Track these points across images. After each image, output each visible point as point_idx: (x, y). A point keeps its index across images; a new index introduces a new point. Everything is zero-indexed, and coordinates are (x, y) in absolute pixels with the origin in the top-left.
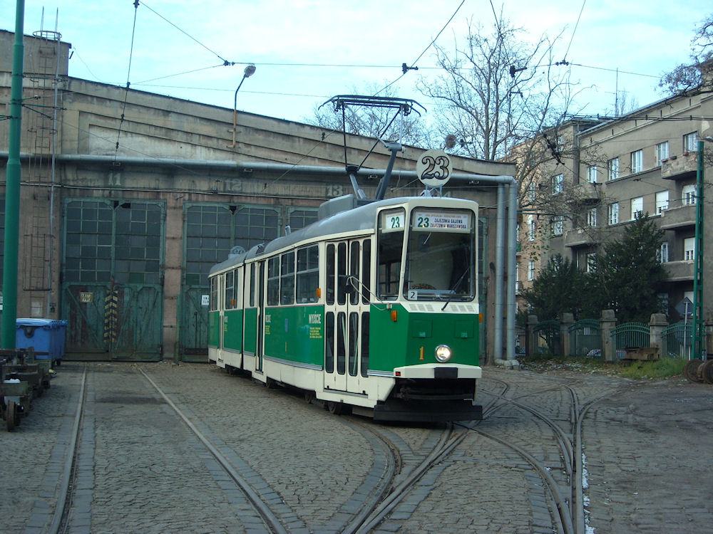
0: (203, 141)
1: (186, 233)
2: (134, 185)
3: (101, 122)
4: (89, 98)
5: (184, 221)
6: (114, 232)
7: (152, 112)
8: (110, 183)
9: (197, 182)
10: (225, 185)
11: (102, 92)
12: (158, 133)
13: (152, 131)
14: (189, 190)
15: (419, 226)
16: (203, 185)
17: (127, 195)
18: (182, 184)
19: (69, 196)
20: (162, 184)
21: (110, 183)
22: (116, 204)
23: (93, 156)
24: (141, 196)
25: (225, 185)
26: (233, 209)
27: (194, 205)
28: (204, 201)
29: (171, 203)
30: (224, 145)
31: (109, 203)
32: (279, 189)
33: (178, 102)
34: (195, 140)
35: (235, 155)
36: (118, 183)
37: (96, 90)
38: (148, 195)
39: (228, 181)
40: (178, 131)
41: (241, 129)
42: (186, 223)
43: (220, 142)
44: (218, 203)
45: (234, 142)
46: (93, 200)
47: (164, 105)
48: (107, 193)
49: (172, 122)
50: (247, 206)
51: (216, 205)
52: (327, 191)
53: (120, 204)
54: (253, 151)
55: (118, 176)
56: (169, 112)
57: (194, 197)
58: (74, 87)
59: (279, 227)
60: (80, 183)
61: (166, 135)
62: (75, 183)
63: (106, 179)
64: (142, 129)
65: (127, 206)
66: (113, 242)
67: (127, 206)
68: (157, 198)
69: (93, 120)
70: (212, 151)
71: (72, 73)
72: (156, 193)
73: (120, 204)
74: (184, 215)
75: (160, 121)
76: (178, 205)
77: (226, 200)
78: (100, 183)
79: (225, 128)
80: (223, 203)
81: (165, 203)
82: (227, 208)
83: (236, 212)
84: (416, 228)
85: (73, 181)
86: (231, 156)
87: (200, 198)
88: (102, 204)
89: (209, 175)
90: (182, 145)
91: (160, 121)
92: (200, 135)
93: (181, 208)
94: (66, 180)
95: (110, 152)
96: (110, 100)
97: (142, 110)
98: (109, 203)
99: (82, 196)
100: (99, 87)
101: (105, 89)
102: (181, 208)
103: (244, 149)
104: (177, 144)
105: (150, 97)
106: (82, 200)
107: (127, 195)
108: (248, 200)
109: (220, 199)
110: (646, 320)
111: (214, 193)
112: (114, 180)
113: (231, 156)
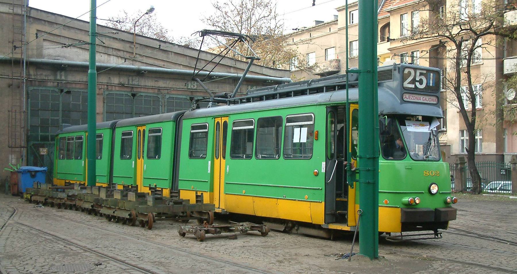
0: (115, 53)
1: (105, 111)
2: (74, 79)
3: (51, 38)
4: (43, 22)
5: (104, 103)
6: (61, 109)
8: (58, 78)
9: (112, 79)
10: (129, 80)
11: (52, 19)
14: (107, 83)
16: (116, 80)
17: (69, 86)
19: (32, 85)
21: (58, 78)
22: (62, 91)
23: (45, 60)
24: (78, 86)
25: (129, 80)
26: (134, 95)
27: (110, 92)
28: (115, 90)
30: (127, 56)
31: (57, 90)
32: (161, 84)
33: (100, 27)
34: (110, 52)
35: (134, 62)
36: (63, 78)
37: (48, 17)
38: (82, 86)
39: (130, 78)
41: (137, 46)
42: (105, 104)
43: (125, 53)
44: (125, 91)
45: (134, 54)
46: (48, 89)
48: (56, 84)
50: (142, 94)
51: (124, 93)
53: (65, 90)
54: (145, 60)
55: (63, 73)
57: (110, 88)
58: (33, 14)
59: (160, 106)
60: (39, 77)
62: (36, 77)
63: (56, 75)
65: (69, 92)
67: (69, 92)
69: (46, 36)
70: (120, 59)
71: (30, 6)
74: (104, 98)
76: (100, 93)
77: (129, 90)
78: (51, 77)
79: (128, 45)
80: (128, 92)
82: (130, 94)
83: (136, 98)
85: (34, 75)
86: (131, 62)
87: (114, 88)
88: (53, 91)
89: (119, 74)
90: (102, 54)
92: (113, 48)
93: (102, 94)
95: (57, 58)
96: (57, 24)
97: (78, 31)
98: (57, 90)
99: (40, 86)
100: (50, 15)
101: (53, 17)
102: (102, 94)
103: (139, 58)
105: (82, 23)
106: (40, 88)
107: (69, 86)
108: (142, 90)
109: (125, 89)
111: (122, 85)
112: (61, 76)
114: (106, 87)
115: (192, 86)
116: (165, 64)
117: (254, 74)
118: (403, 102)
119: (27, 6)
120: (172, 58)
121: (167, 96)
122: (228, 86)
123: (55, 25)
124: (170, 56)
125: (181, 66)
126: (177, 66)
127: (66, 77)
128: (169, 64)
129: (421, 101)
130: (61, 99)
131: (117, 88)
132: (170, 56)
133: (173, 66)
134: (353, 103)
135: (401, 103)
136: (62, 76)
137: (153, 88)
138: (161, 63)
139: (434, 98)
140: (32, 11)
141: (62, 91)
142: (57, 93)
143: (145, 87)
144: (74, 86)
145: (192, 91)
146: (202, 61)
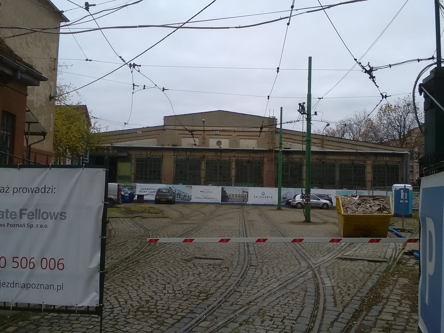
30: (319, 145)
36: (290, 157)
48: (287, 159)
52: (350, 158)
54: (328, 147)
64: (296, 141)
72: (301, 159)
73: (291, 162)
88: (286, 162)
97: (297, 136)
111: (317, 159)
113: (321, 148)
115: (352, 158)
117: (384, 150)
119: (276, 128)
121: (339, 163)
131: (315, 160)
137: (333, 159)
140: (278, 129)
143: (328, 159)
145: (353, 160)
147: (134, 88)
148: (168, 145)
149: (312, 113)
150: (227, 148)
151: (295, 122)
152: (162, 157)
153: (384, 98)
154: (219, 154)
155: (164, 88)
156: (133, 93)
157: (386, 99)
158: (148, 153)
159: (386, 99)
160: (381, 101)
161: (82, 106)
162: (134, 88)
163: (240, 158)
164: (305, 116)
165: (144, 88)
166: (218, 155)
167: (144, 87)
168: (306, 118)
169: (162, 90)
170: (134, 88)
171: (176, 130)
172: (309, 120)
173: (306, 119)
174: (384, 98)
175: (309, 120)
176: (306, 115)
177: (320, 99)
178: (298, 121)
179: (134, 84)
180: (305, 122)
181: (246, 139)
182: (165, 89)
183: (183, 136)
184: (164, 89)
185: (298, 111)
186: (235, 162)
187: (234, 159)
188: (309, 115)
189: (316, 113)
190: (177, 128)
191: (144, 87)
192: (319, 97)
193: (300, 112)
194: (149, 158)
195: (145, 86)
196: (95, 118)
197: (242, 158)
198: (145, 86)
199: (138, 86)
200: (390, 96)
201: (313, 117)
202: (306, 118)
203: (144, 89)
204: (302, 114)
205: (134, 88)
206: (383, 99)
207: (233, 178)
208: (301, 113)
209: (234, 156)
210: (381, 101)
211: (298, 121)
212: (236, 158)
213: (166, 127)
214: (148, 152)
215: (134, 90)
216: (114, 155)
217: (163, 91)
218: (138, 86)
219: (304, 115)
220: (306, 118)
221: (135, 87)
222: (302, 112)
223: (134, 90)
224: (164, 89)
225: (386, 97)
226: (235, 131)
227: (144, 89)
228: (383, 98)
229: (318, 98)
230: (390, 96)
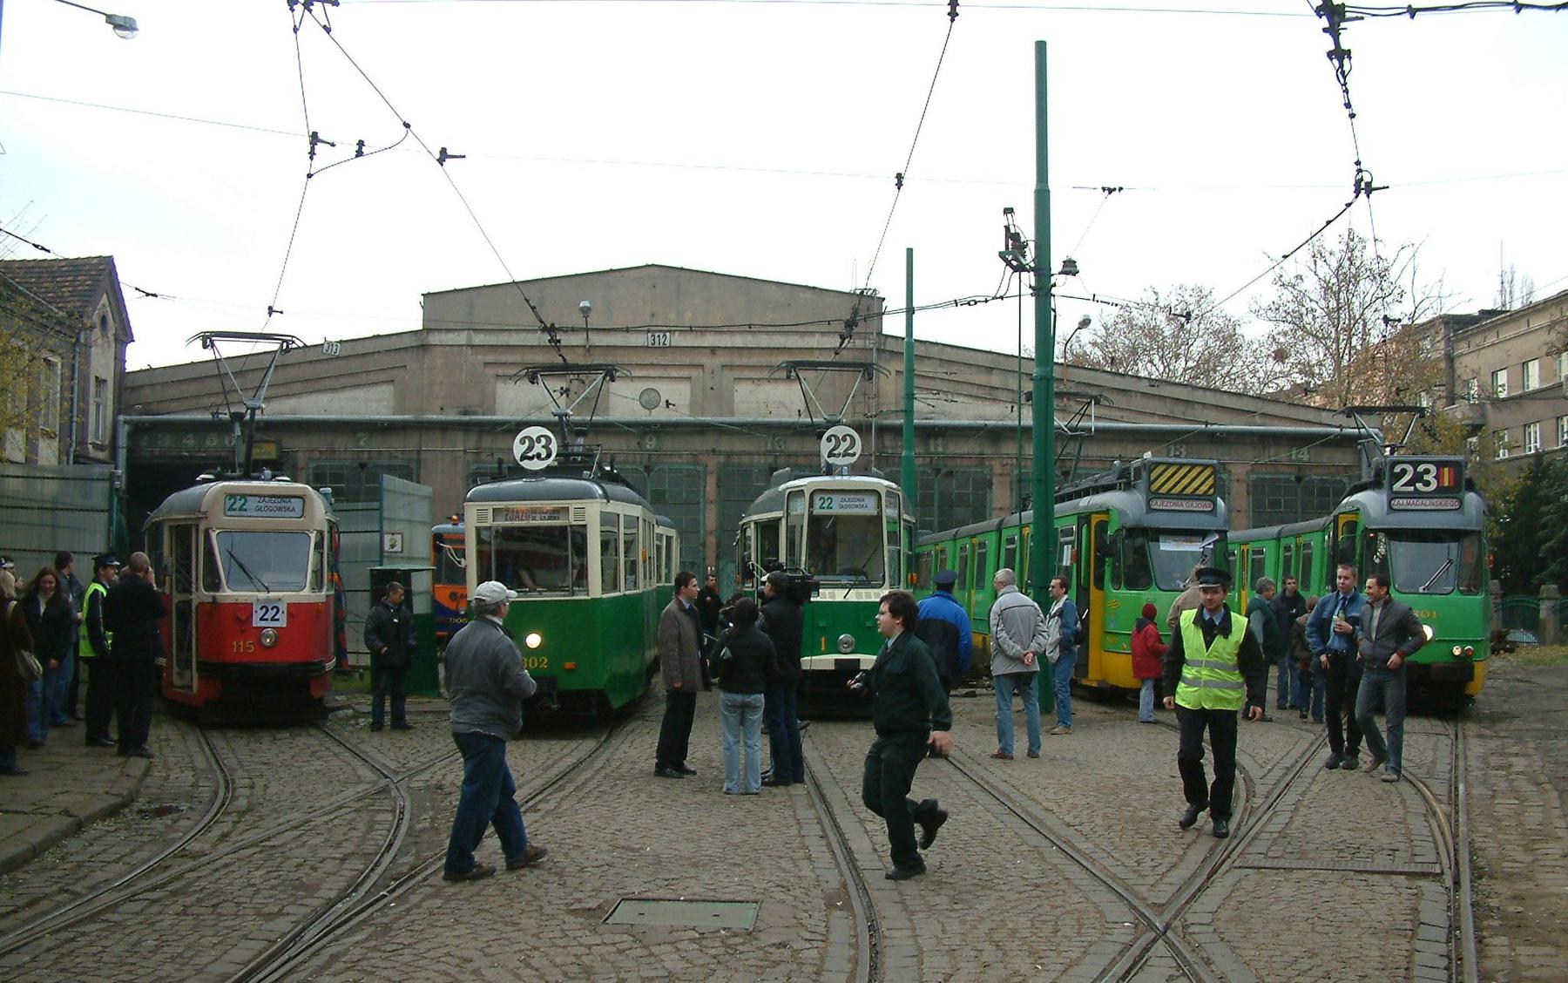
6: (936, 505)
7: (974, 370)
8: (932, 449)
12: (981, 392)
13: (974, 391)
15: (821, 508)
17: (950, 463)
18: (1009, 448)
20: (988, 450)
21: (932, 449)
22: (938, 471)
24: (965, 462)
29: (997, 469)
31: (930, 471)
33: (1002, 357)
36: (940, 449)
38: (974, 462)
40: (1003, 389)
47: (987, 361)
49: (995, 380)
53: (943, 471)
55: (940, 441)
56: (993, 369)
61: (990, 394)
62: (894, 451)
63: (927, 445)
66: (936, 514)
68: (982, 465)
71: (885, 332)
72: (981, 459)
73: (943, 471)
74: (1011, 482)
75: (982, 379)
81: (991, 470)
84: (817, 511)
85: (892, 448)
91: (982, 379)
93: (1008, 475)
94: (884, 447)
95: (929, 416)
96: (929, 358)
102: (1008, 475)
104: (1002, 404)
105: (972, 353)
107: (950, 463)
110: (1535, 591)
114: (1014, 460)
116: (1125, 414)
118: (1150, 510)
119: (880, 333)
120: (1138, 403)
122: (1249, 449)
123: (926, 361)
124: (1134, 399)
125: (1156, 417)
126: (1147, 418)
127: (945, 446)
128: (1132, 415)
129: (1185, 508)
130: (936, 485)
132: (1134, 399)
133: (1140, 417)
134: (1096, 513)
135: (1147, 513)
136: (937, 447)
138: (1118, 414)
139: (1208, 503)
140: (889, 339)
141: (938, 471)
142: (930, 475)
144: (958, 461)
146: (1196, 406)
147: (312, 154)
148: (442, 409)
149: (1056, 265)
150: (681, 414)
151: (986, 301)
152: (419, 461)
153: (1363, 194)
154: (650, 444)
155: (443, 151)
156: (310, 176)
157: (1368, 196)
158: (361, 443)
159: (1368, 196)
160: (1348, 205)
161: (95, 261)
162: (312, 154)
163: (735, 459)
164: (1029, 278)
165: (359, 154)
166: (648, 447)
167: (360, 148)
168: (1030, 287)
169: (438, 156)
170: (313, 149)
171: (473, 346)
172: (1043, 293)
173: (1031, 291)
174: (1363, 194)
175: (1043, 293)
176: (1032, 273)
177: (1111, 191)
178: (1002, 298)
179: (315, 135)
180: (1029, 303)
181: (759, 380)
182: (449, 153)
183: (501, 371)
184: (444, 156)
185: (1002, 255)
186: (715, 476)
187: (712, 463)
188: (1042, 271)
189: (1070, 268)
190: (478, 339)
191: (360, 148)
192: (1106, 185)
193: (1008, 263)
194: (363, 466)
195: (361, 144)
196: (148, 295)
197: (746, 459)
198: (361, 144)
199: (333, 145)
200: (1384, 188)
201: (1063, 286)
202: (1033, 284)
203: (357, 156)
204: (1015, 269)
205: (313, 149)
206: (1357, 197)
207: (712, 540)
208: (1012, 266)
209: (713, 451)
210: (1348, 205)
211: (1002, 298)
212: (722, 459)
213: (435, 339)
214: (361, 438)
215: (311, 158)
216: (223, 454)
217: (441, 161)
218: (333, 145)
219: (1024, 274)
220: (1033, 284)
221: (319, 148)
222: (1014, 263)
223: (311, 158)
224: (444, 156)
225: (1369, 190)
226: (713, 350)
227: (357, 156)
228: (1357, 192)
229: (1104, 189)
230: (1384, 188)
